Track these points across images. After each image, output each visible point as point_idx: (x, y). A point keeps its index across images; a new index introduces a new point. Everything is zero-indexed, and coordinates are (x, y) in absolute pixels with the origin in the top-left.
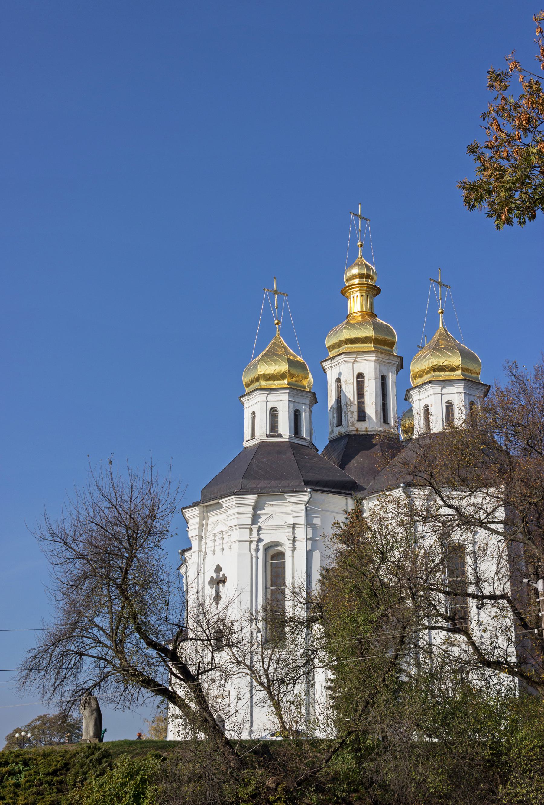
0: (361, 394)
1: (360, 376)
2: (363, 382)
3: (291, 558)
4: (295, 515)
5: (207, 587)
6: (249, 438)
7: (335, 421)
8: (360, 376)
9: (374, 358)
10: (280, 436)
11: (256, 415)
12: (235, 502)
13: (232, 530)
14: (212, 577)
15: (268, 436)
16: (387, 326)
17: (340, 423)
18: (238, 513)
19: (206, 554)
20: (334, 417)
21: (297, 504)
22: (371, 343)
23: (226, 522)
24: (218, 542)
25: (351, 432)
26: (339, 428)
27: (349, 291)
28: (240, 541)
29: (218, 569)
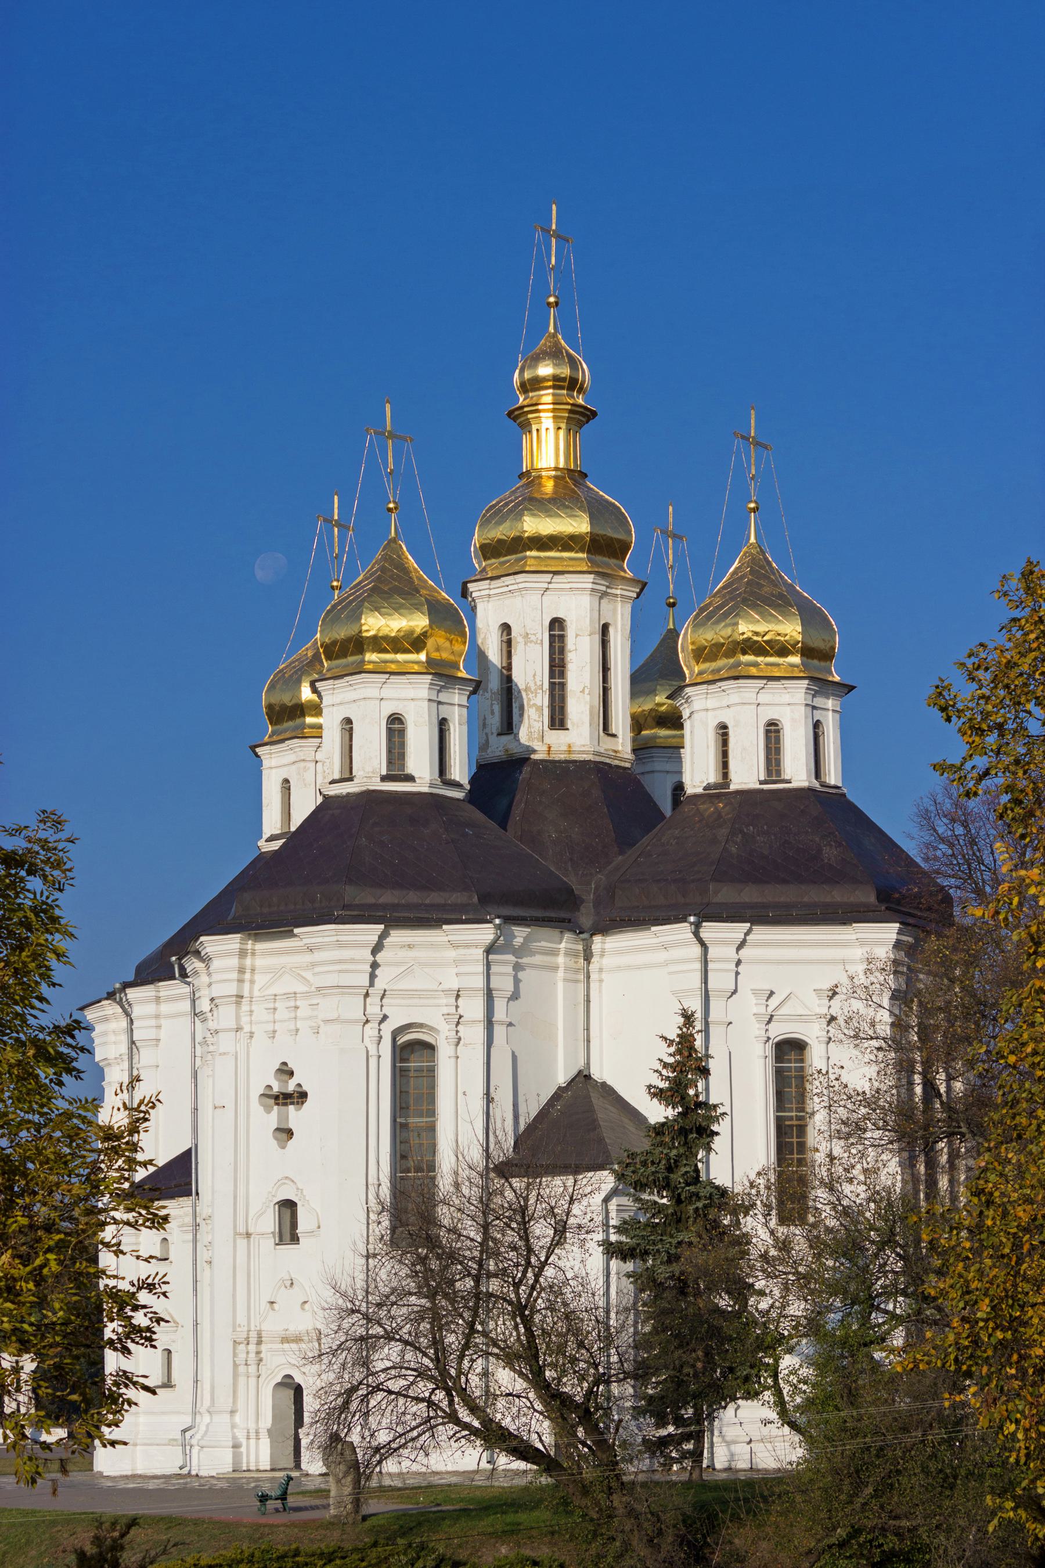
0: (557, 666)
1: (557, 624)
2: (562, 638)
4: (463, 969)
6: (337, 776)
8: (557, 624)
9: (590, 586)
10: (410, 778)
11: (355, 726)
12: (335, 938)
13: (324, 995)
15: (384, 779)
16: (613, 504)
18: (340, 962)
19: (251, 1035)
20: (493, 713)
21: (467, 946)
22: (582, 550)
23: (308, 975)
24: (282, 1013)
26: (505, 739)
27: (530, 416)
29: (285, 1071)
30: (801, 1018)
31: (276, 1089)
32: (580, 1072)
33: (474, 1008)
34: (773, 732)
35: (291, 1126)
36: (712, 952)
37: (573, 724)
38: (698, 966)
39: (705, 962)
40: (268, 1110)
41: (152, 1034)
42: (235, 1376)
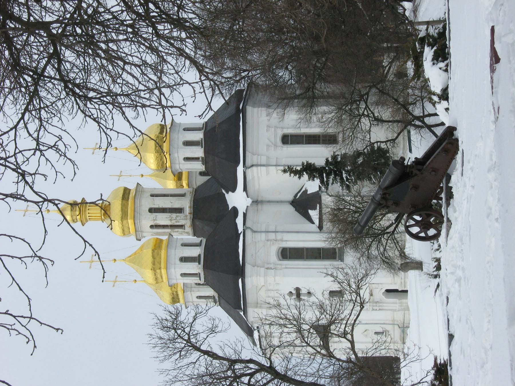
0: (163, 210)
1: (151, 210)
3: (288, 242)
6: (198, 278)
7: (180, 230)
8: (151, 210)
10: (200, 255)
15: (199, 263)
17: (182, 226)
25: (191, 217)
26: (186, 227)
30: (275, 136)
31: (295, 297)
32: (291, 204)
33: (272, 236)
34: (187, 143)
36: (255, 163)
37: (182, 206)
38: (259, 168)
39: (257, 165)
42: (383, 309)
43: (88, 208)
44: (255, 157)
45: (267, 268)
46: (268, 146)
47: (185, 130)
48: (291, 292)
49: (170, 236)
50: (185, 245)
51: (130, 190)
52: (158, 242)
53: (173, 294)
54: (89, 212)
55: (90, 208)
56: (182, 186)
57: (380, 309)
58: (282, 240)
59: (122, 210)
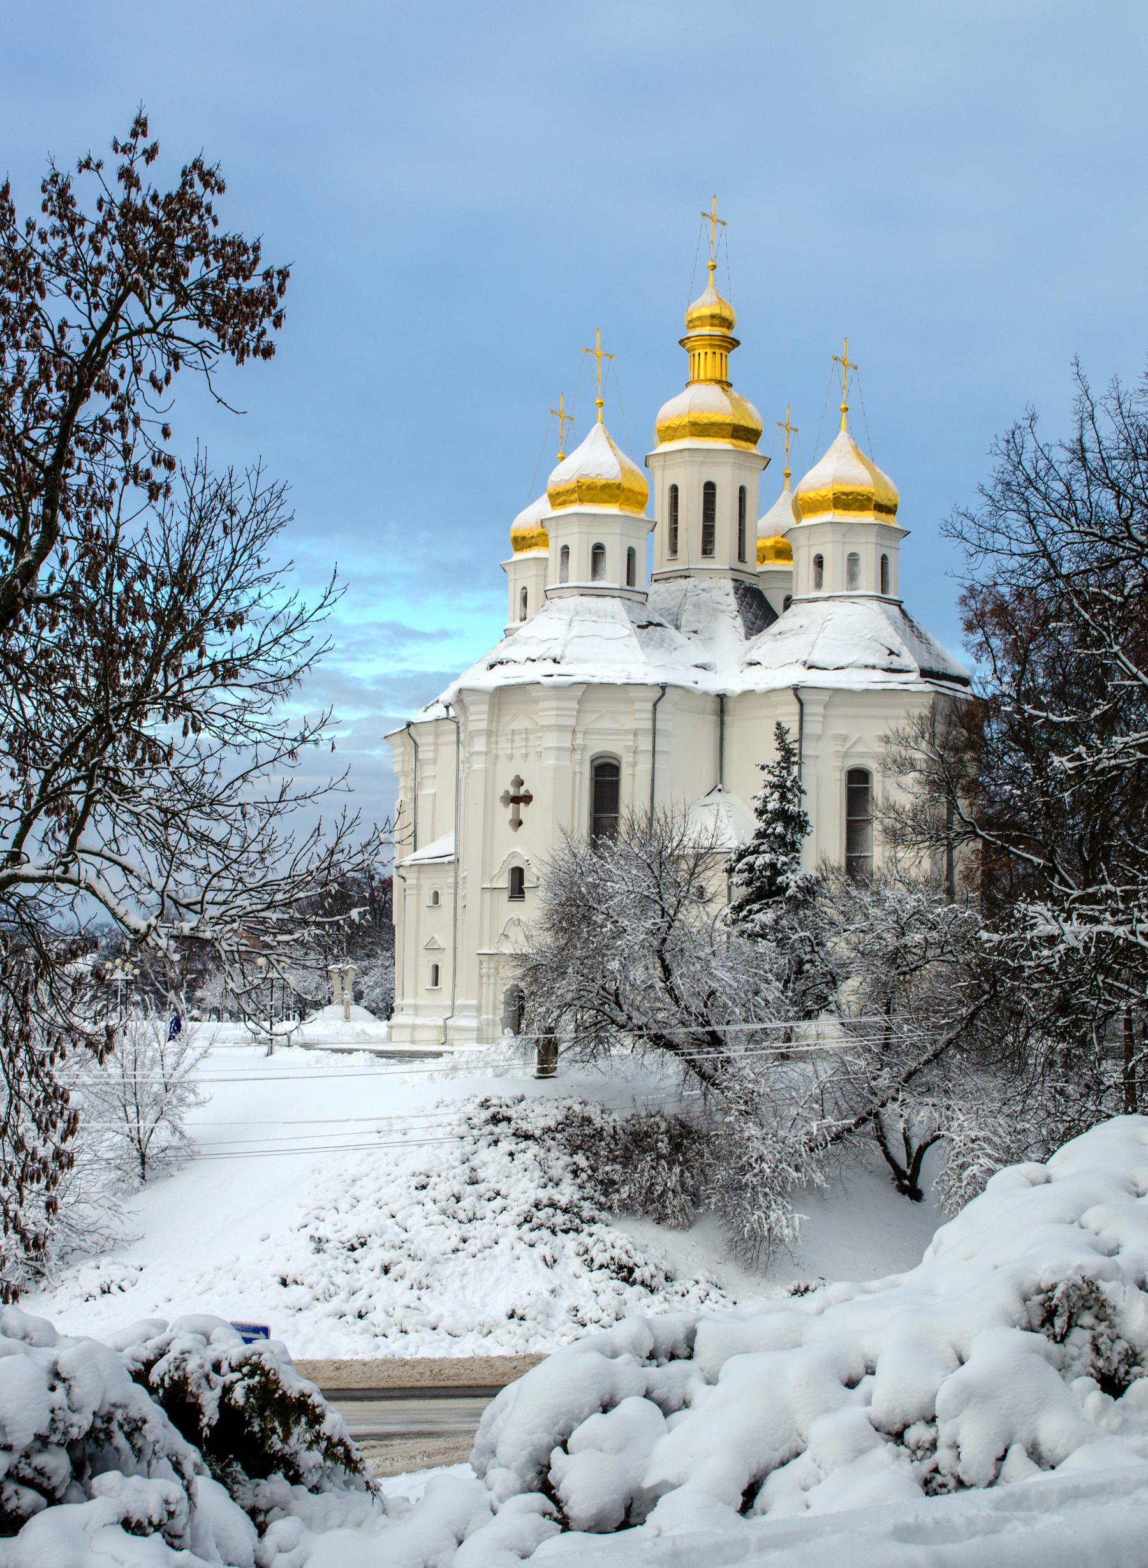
1: (710, 489)
5: (500, 806)
8: (710, 489)
14: (507, 792)
28: (558, 749)
29: (519, 782)
31: (512, 793)
33: (645, 744)
35: (521, 817)
36: (807, 709)
40: (507, 805)
41: (431, 755)
42: (481, 984)
43: (718, 351)
44: (820, 709)
45: (574, 732)
46: (845, 738)
47: (884, 558)
48: (522, 784)
49: (650, 526)
50: (631, 554)
51: (755, 443)
52: (640, 497)
53: (533, 537)
54: (709, 356)
55: (718, 356)
56: (762, 559)
57: (481, 977)
58: (634, 764)
59: (712, 424)
